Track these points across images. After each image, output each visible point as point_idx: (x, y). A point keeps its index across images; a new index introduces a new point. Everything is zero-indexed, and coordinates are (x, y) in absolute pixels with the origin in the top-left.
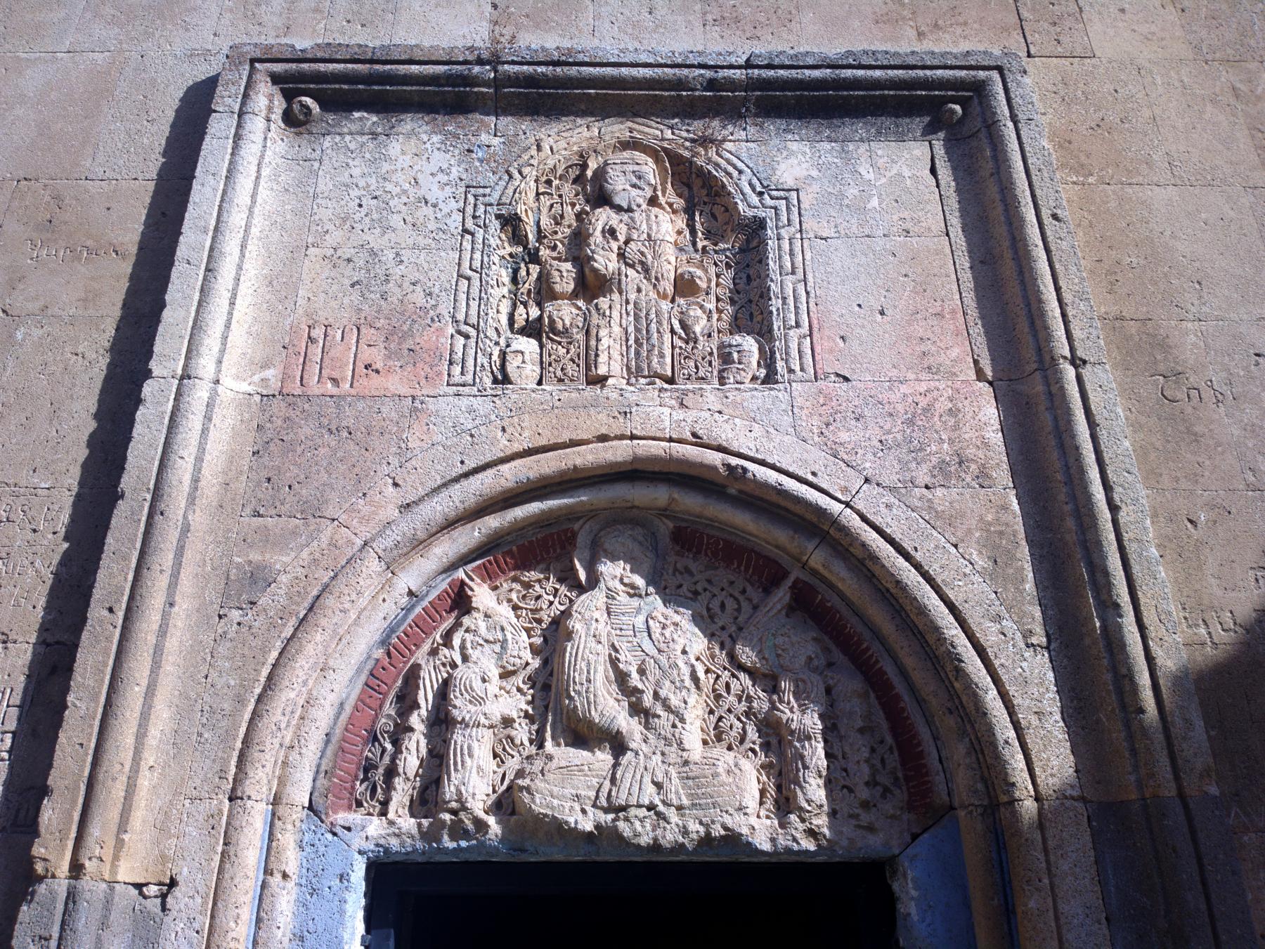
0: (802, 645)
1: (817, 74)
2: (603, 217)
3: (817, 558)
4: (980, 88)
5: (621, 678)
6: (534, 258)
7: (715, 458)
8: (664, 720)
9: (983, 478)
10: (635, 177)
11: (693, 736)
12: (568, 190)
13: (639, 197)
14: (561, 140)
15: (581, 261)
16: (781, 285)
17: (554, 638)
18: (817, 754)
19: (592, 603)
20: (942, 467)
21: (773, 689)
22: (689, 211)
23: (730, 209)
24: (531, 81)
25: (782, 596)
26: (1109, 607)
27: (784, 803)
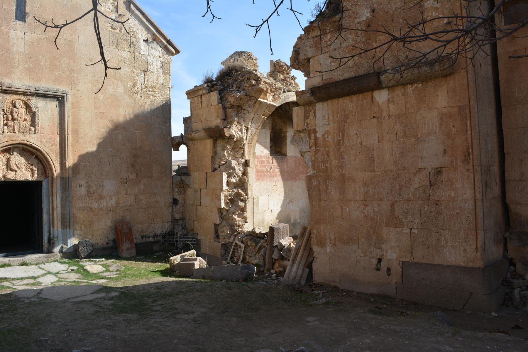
0: (36, 161)
1: (44, 92)
2: (15, 109)
3: (38, 153)
4: (64, 96)
5: (16, 165)
6: (6, 114)
7: (28, 143)
8: (21, 169)
9: (56, 146)
10: (19, 104)
11: (24, 170)
12: (10, 104)
13: (20, 107)
14: (10, 98)
15: (13, 116)
16: (37, 121)
17: (8, 160)
18: (36, 172)
19: (13, 157)
20: (52, 145)
21: (32, 166)
22: (26, 108)
23: (31, 110)
24: (6, 90)
25: (34, 156)
26: (66, 160)
27: (33, 176)
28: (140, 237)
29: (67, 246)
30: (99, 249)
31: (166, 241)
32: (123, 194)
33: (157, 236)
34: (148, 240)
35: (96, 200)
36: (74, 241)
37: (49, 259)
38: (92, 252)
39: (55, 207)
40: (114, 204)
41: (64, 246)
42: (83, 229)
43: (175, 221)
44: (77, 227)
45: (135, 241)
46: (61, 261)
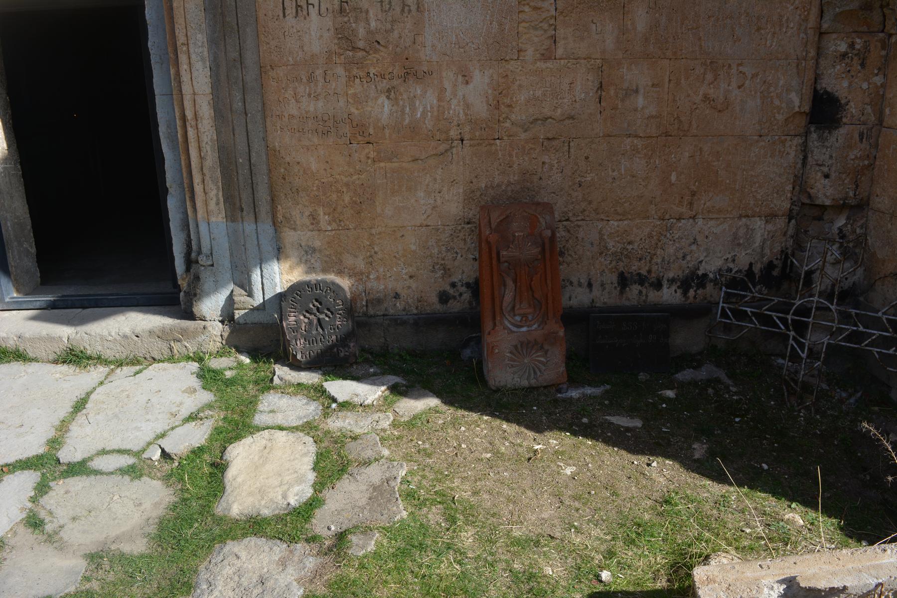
28: (614, 278)
29: (250, 294)
30: (397, 322)
31: (740, 315)
32: (529, 54)
33: (702, 280)
34: (653, 296)
35: (384, 84)
36: (278, 277)
37: (176, 347)
38: (343, 341)
39: (189, 114)
40: (480, 109)
41: (240, 297)
42: (323, 225)
43: (806, 212)
44: (295, 213)
45: (578, 297)
46: (216, 363)
